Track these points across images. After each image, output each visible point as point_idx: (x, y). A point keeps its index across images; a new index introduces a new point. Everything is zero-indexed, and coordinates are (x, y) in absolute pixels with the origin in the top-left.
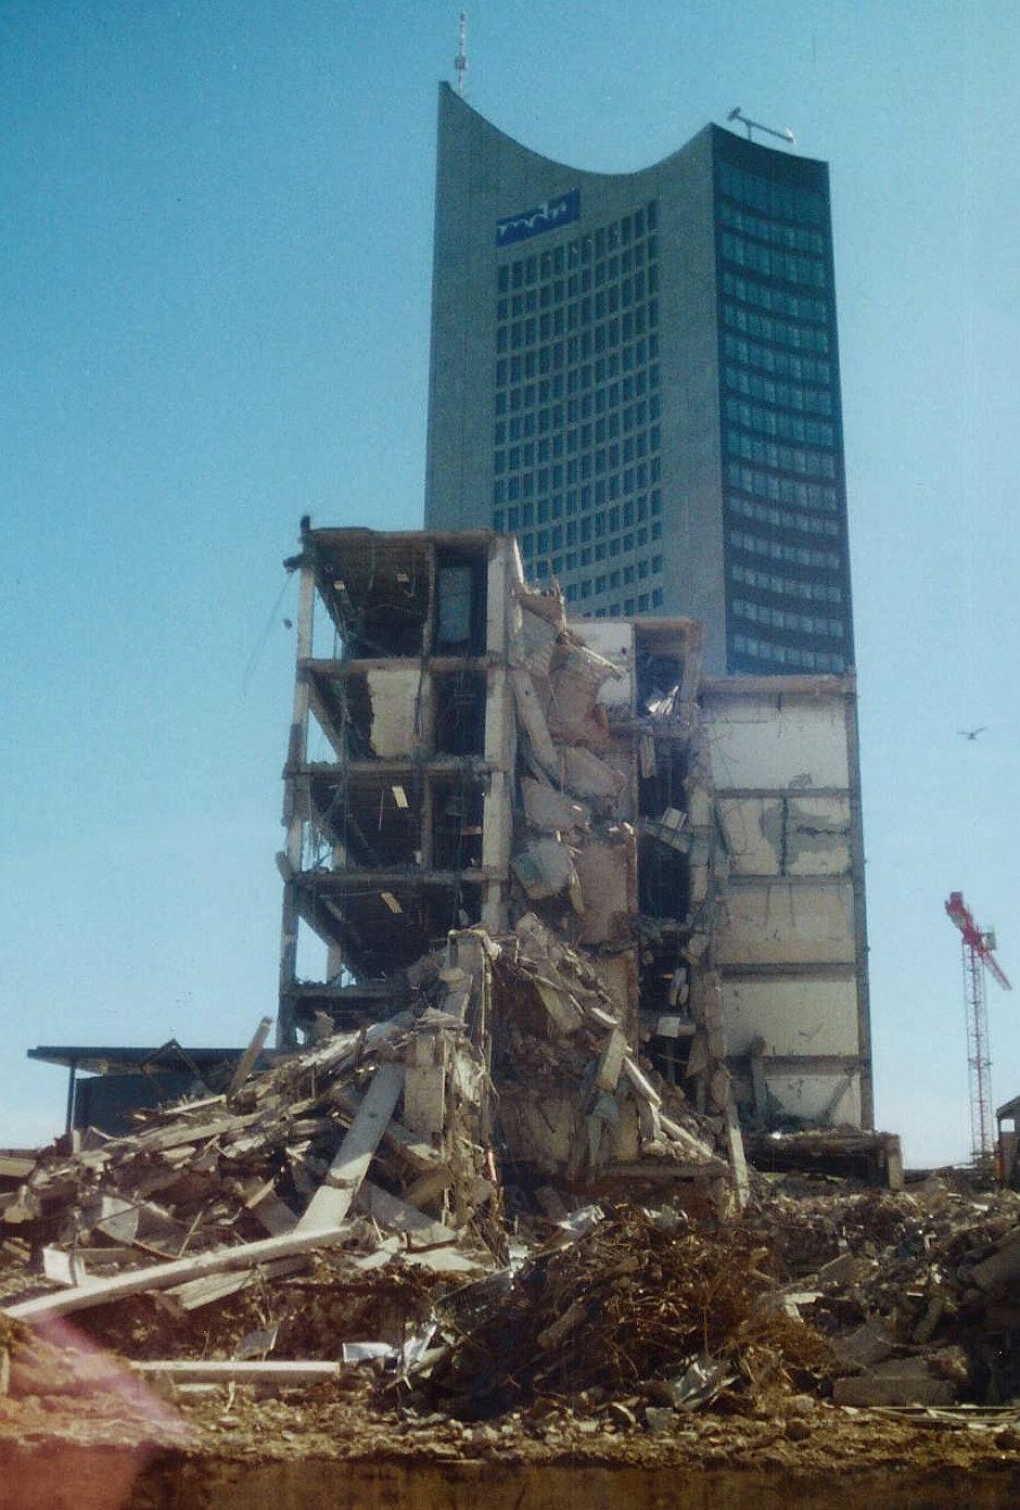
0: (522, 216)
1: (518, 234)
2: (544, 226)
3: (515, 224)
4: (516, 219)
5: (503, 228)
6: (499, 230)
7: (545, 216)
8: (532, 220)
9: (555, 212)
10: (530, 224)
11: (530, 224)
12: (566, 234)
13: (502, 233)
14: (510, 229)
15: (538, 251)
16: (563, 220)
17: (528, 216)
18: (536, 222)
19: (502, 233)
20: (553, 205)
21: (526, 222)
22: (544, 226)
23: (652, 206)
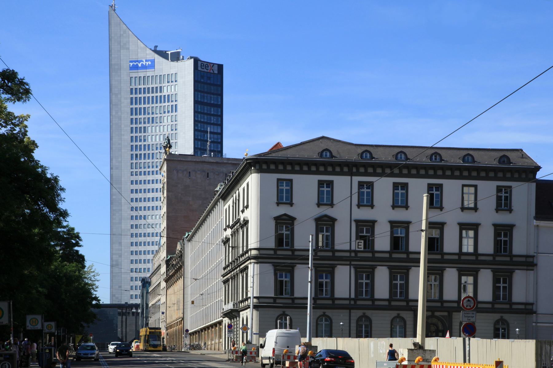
0: (137, 61)
1: (135, 68)
4: (135, 62)
5: (131, 64)
7: (144, 64)
10: (140, 66)
11: (140, 66)
12: (150, 73)
15: (142, 76)
17: (139, 62)
18: (142, 64)
20: (146, 61)
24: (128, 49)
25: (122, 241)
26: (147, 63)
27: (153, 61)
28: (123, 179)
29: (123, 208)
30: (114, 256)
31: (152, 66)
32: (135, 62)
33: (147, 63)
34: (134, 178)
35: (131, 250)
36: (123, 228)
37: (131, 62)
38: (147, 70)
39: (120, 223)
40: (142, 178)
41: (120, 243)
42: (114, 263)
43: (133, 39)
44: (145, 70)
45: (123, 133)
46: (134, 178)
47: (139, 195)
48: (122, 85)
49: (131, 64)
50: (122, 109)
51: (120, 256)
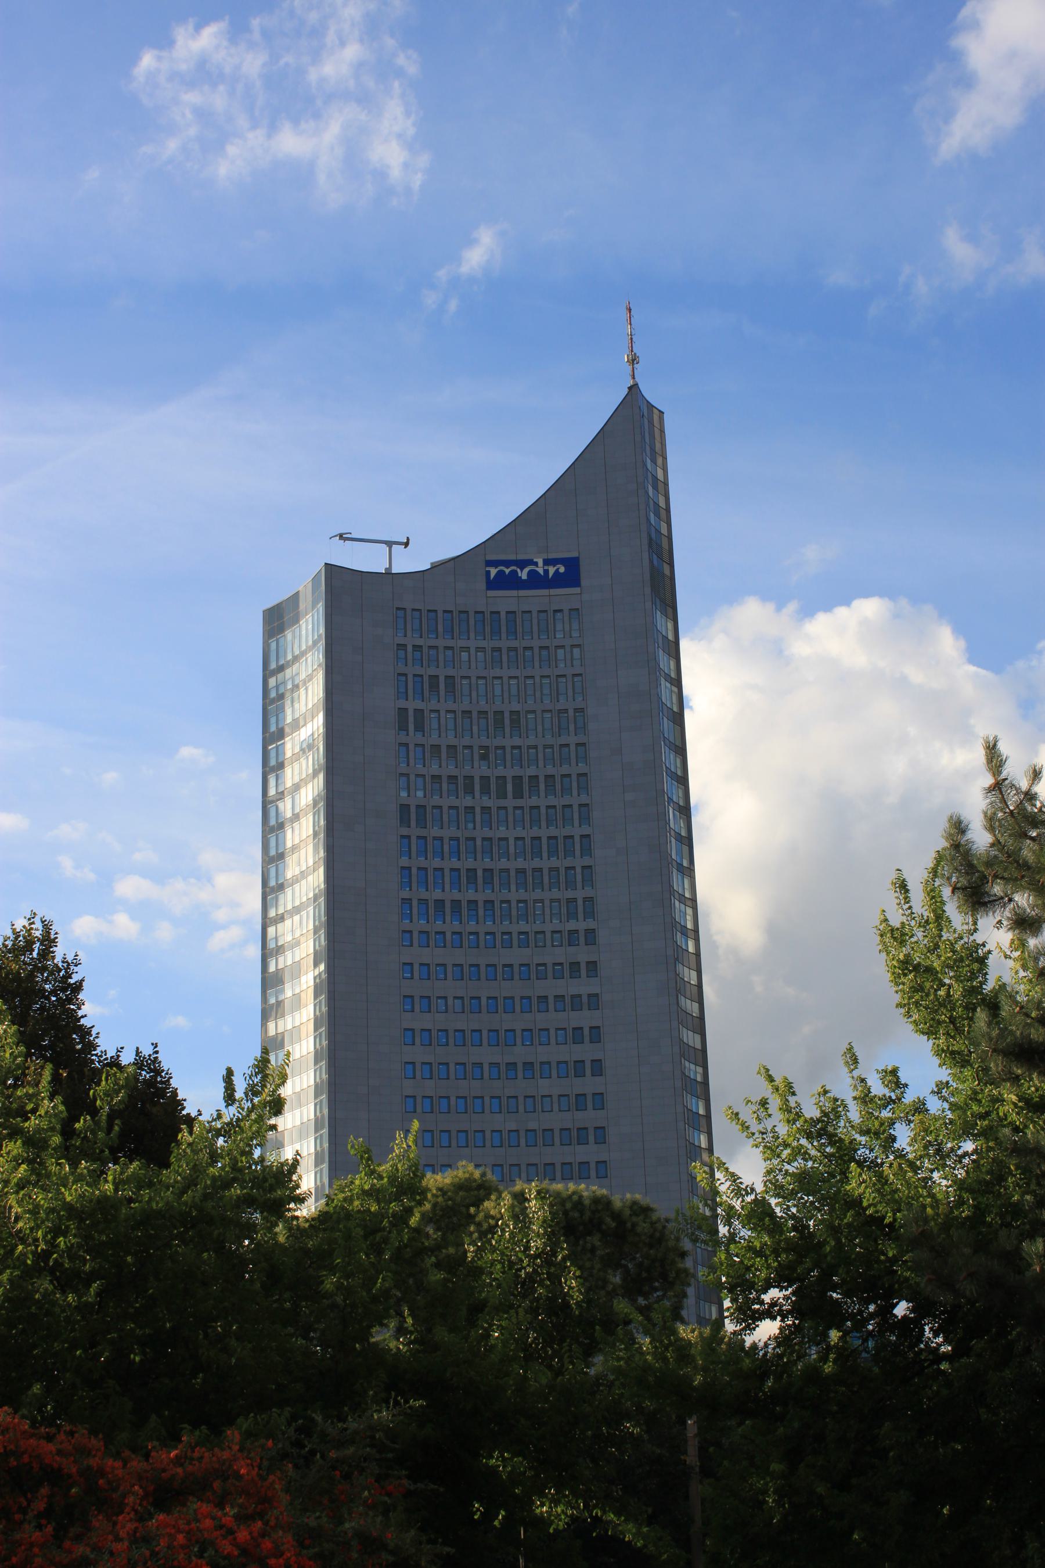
2: (536, 581)
3: (507, 571)
4: (507, 563)
5: (493, 572)
6: (488, 573)
7: (541, 571)
8: (526, 570)
9: (552, 570)
10: (524, 577)
11: (524, 577)
13: (492, 576)
14: (501, 573)
16: (558, 581)
17: (522, 564)
18: (530, 573)
19: (492, 576)
20: (547, 562)
21: (519, 570)
27: (573, 565)
33: (552, 570)
38: (553, 592)
44: (545, 592)
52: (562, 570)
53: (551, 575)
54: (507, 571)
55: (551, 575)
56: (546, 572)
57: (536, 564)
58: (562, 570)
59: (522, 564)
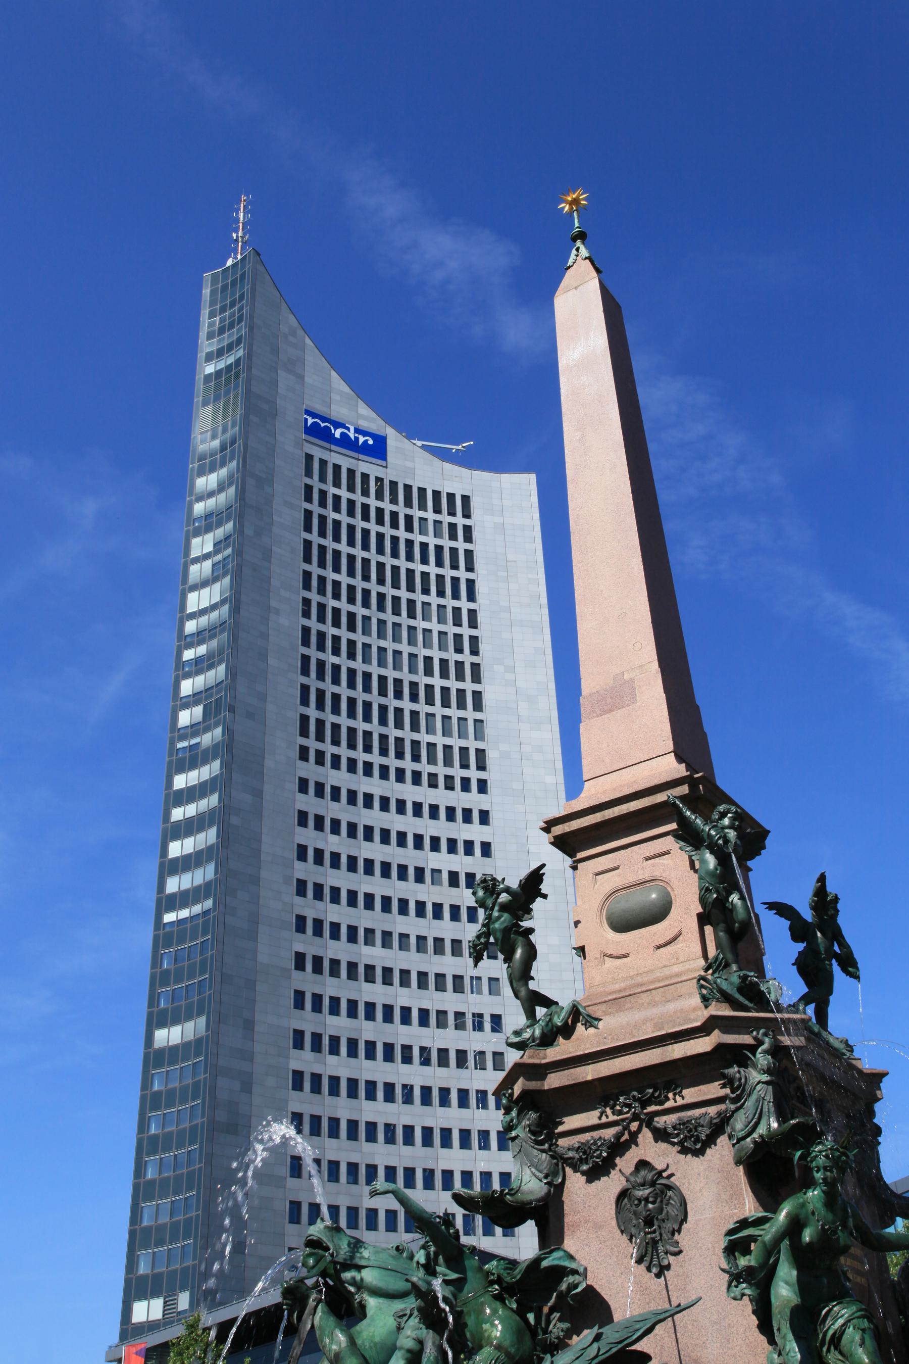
2: (346, 442)
3: (323, 425)
4: (324, 419)
5: (310, 421)
6: (306, 420)
7: (352, 435)
10: (338, 433)
11: (338, 433)
13: (309, 424)
16: (365, 450)
17: (338, 425)
18: (342, 434)
19: (309, 424)
20: (357, 431)
22: (346, 442)
23: (466, 499)
24: (302, 377)
25: (258, 1017)
26: (362, 439)
28: (269, 763)
29: (264, 874)
30: (222, 1082)
31: (378, 449)
32: (324, 419)
33: (362, 439)
34: (310, 770)
35: (295, 1065)
36: (263, 957)
37: (308, 412)
38: (361, 457)
39: (253, 936)
40: (341, 778)
41: (249, 1025)
42: (221, 1116)
43: (313, 358)
45: (273, 603)
46: (310, 770)
47: (332, 843)
48: (277, 461)
49: (310, 421)
50: (275, 530)
51: (247, 1087)
52: (371, 442)
53: (360, 443)
54: (323, 425)
55: (360, 443)
56: (357, 439)
57: (348, 429)
58: (371, 442)
59: (338, 425)
